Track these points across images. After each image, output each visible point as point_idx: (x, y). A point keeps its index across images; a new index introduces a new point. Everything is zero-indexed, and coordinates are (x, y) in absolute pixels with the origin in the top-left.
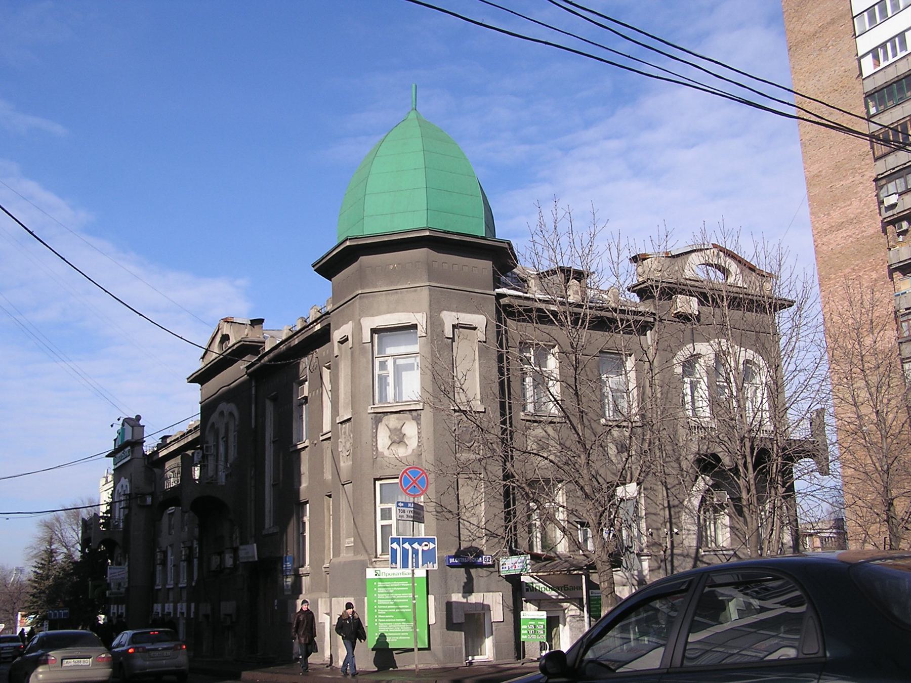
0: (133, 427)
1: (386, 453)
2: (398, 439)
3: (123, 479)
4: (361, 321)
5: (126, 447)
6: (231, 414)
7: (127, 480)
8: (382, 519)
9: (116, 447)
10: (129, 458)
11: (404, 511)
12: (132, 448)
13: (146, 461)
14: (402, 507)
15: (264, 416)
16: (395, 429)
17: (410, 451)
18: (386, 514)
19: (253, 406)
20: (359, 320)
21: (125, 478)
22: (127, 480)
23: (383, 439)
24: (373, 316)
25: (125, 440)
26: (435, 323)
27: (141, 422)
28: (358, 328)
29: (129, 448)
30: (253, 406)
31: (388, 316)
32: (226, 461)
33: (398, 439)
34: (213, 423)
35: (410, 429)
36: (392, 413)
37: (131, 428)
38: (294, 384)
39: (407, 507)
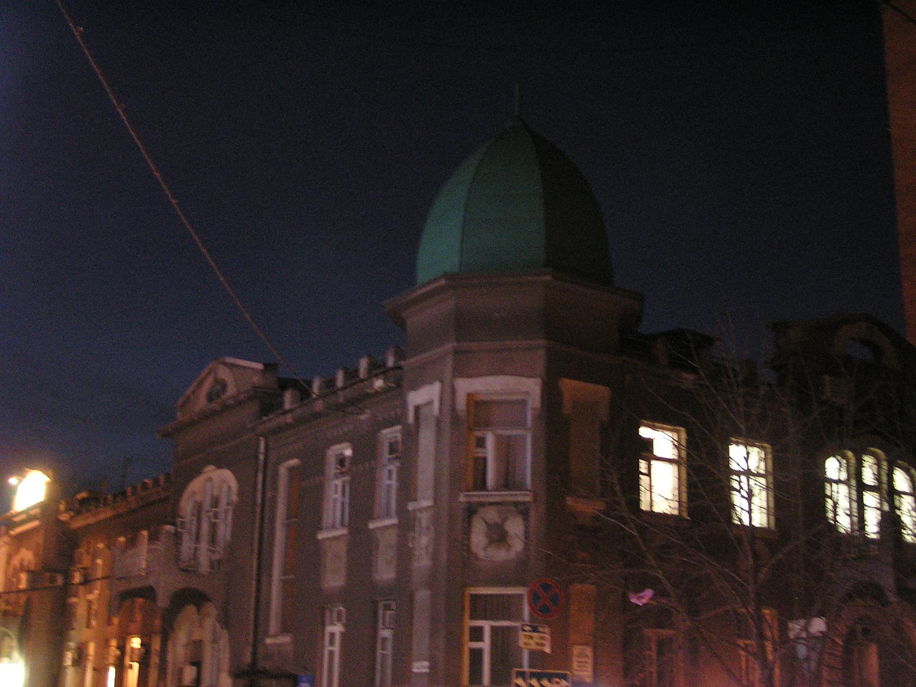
1: (481, 553)
2: (498, 536)
8: (471, 640)
11: (531, 638)
14: (530, 631)
15: (275, 488)
16: (496, 524)
17: (512, 555)
18: (477, 634)
23: (478, 538)
26: (551, 394)
31: (490, 379)
32: (213, 539)
33: (498, 536)
35: (515, 527)
36: (492, 504)
39: (538, 632)
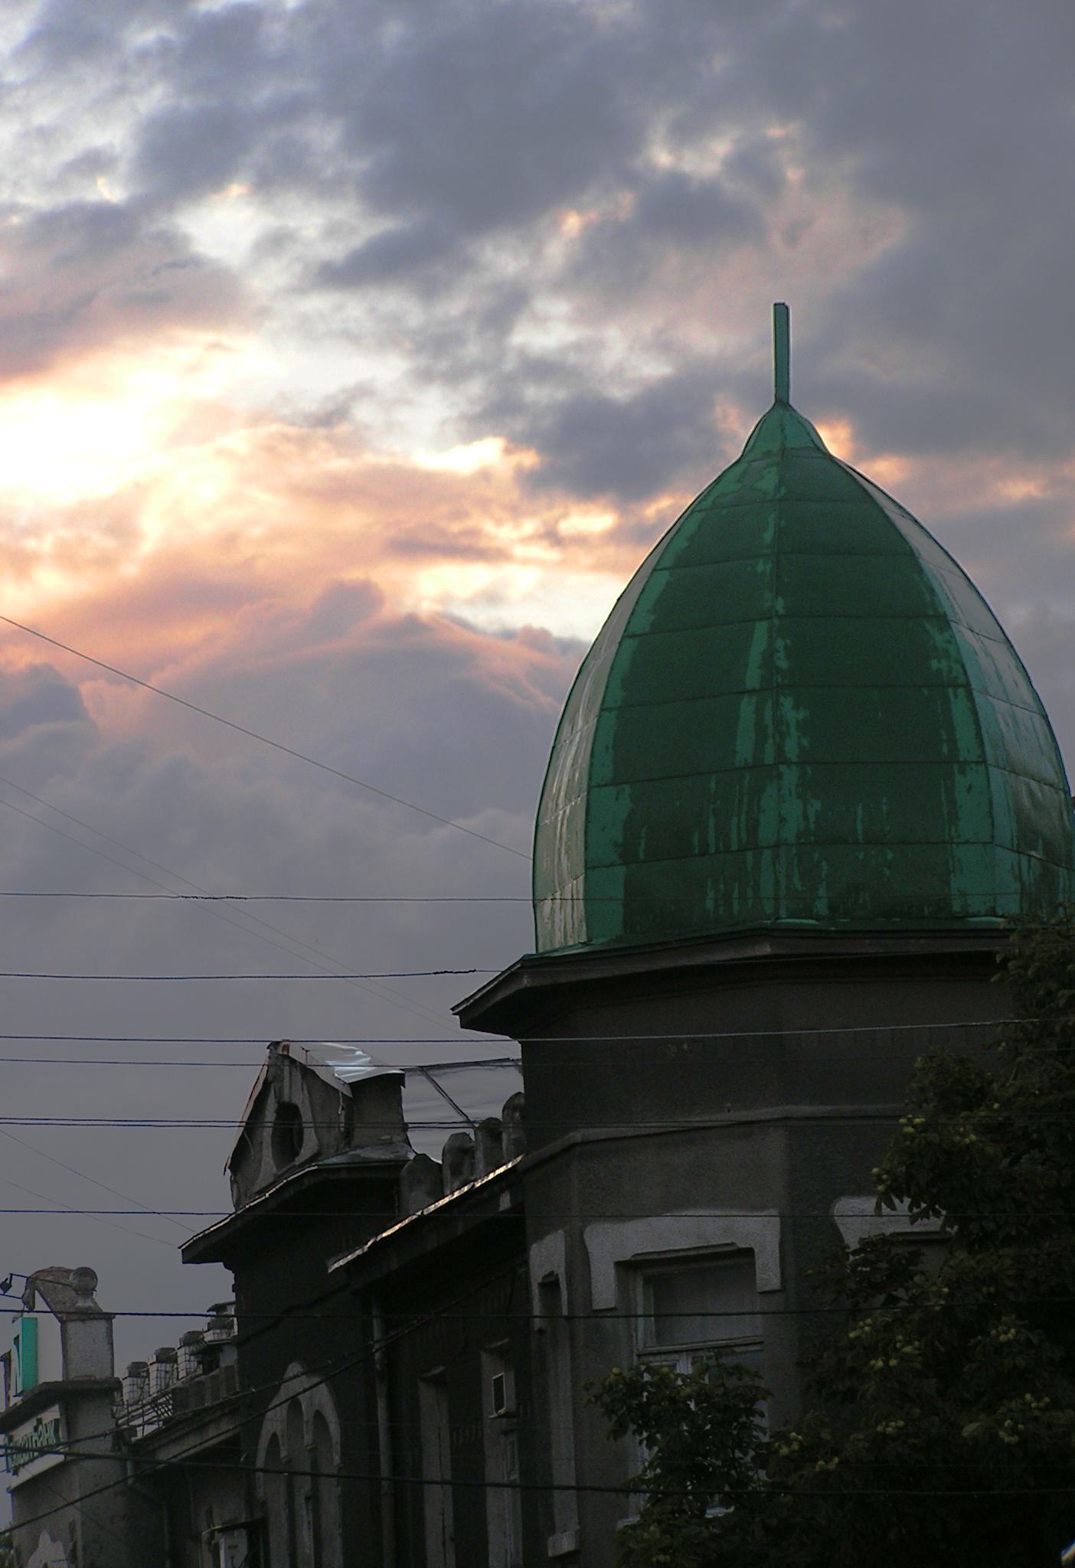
0: (63, 1323)
3: (45, 1539)
4: (586, 1237)
5: (45, 1406)
6: (319, 1416)
7: (60, 1544)
9: (15, 1401)
10: (52, 1460)
12: (69, 1419)
13: (129, 1465)
19: (381, 1405)
20: (582, 1234)
21: (54, 1539)
22: (60, 1544)
24: (621, 1217)
25: (40, 1382)
27: (104, 1299)
28: (579, 1257)
29: (52, 1414)
30: (381, 1405)
34: (274, 1436)
37: (59, 1324)
38: (485, 1357)
